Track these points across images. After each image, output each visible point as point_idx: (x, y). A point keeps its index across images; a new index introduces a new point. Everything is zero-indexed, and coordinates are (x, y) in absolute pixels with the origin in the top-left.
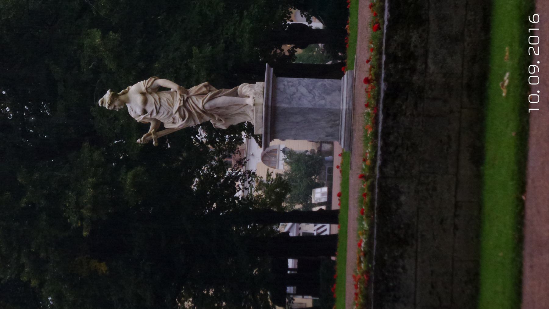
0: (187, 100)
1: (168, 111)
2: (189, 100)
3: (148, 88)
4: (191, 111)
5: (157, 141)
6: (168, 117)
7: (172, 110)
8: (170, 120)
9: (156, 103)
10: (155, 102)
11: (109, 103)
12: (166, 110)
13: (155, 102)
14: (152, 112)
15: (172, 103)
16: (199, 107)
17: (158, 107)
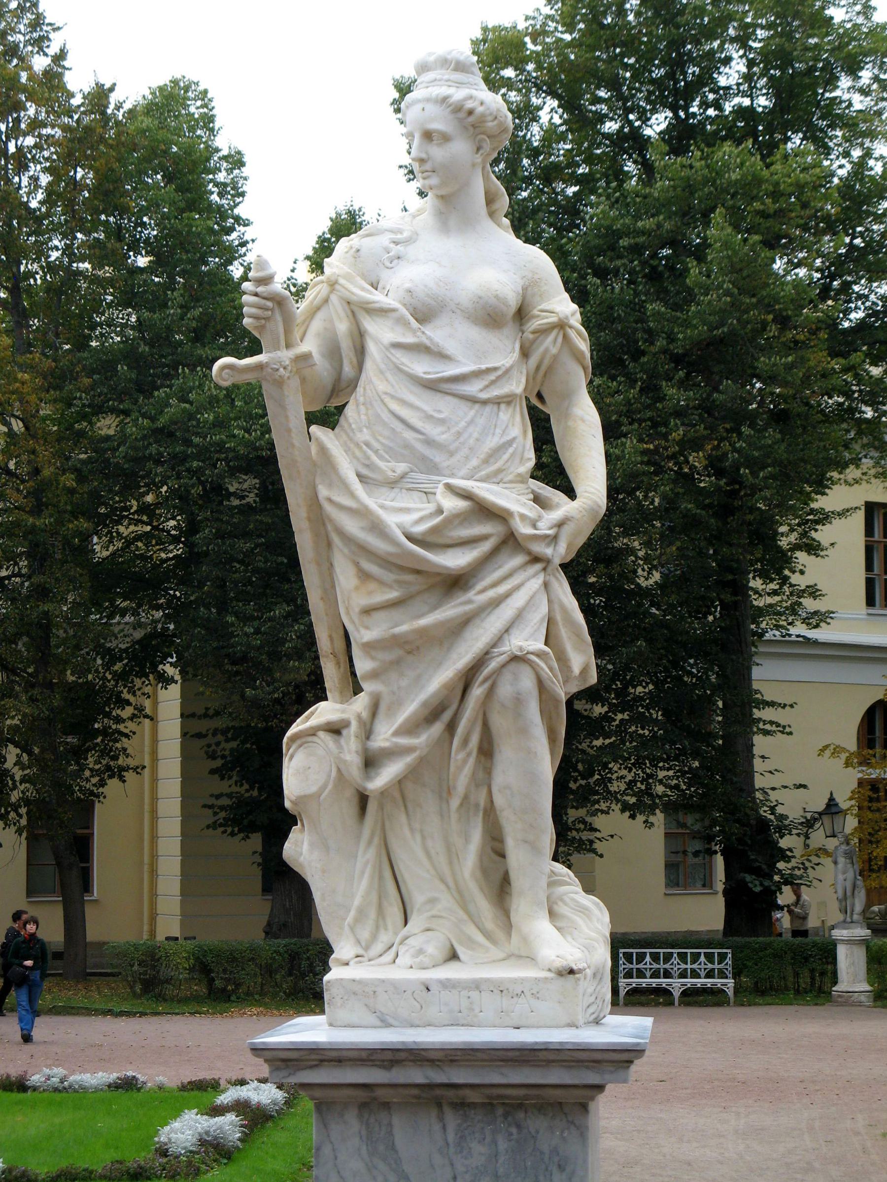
0: (535, 559)
1: (452, 447)
2: (534, 576)
3: (566, 337)
4: (479, 587)
5: (250, 377)
6: (407, 446)
7: (463, 472)
8: (381, 458)
9: (492, 377)
10: (500, 373)
11: (469, 105)
12: (459, 434)
13: (495, 369)
14: (442, 356)
15: (499, 471)
16: (514, 632)
17: (473, 388)
